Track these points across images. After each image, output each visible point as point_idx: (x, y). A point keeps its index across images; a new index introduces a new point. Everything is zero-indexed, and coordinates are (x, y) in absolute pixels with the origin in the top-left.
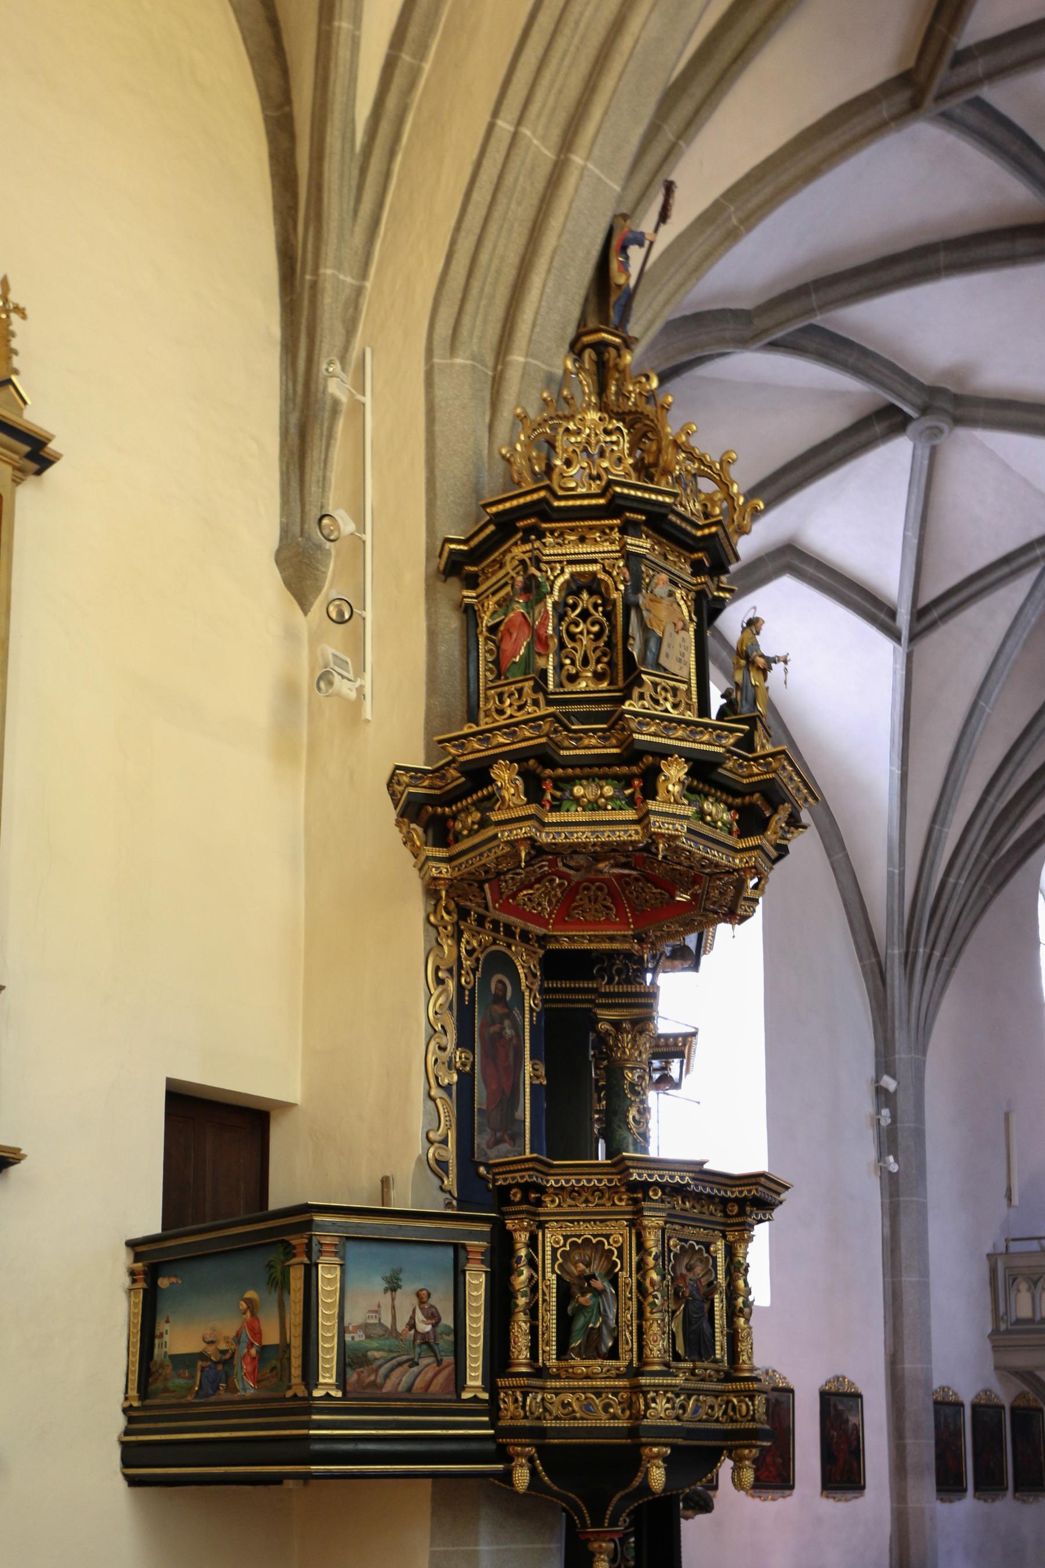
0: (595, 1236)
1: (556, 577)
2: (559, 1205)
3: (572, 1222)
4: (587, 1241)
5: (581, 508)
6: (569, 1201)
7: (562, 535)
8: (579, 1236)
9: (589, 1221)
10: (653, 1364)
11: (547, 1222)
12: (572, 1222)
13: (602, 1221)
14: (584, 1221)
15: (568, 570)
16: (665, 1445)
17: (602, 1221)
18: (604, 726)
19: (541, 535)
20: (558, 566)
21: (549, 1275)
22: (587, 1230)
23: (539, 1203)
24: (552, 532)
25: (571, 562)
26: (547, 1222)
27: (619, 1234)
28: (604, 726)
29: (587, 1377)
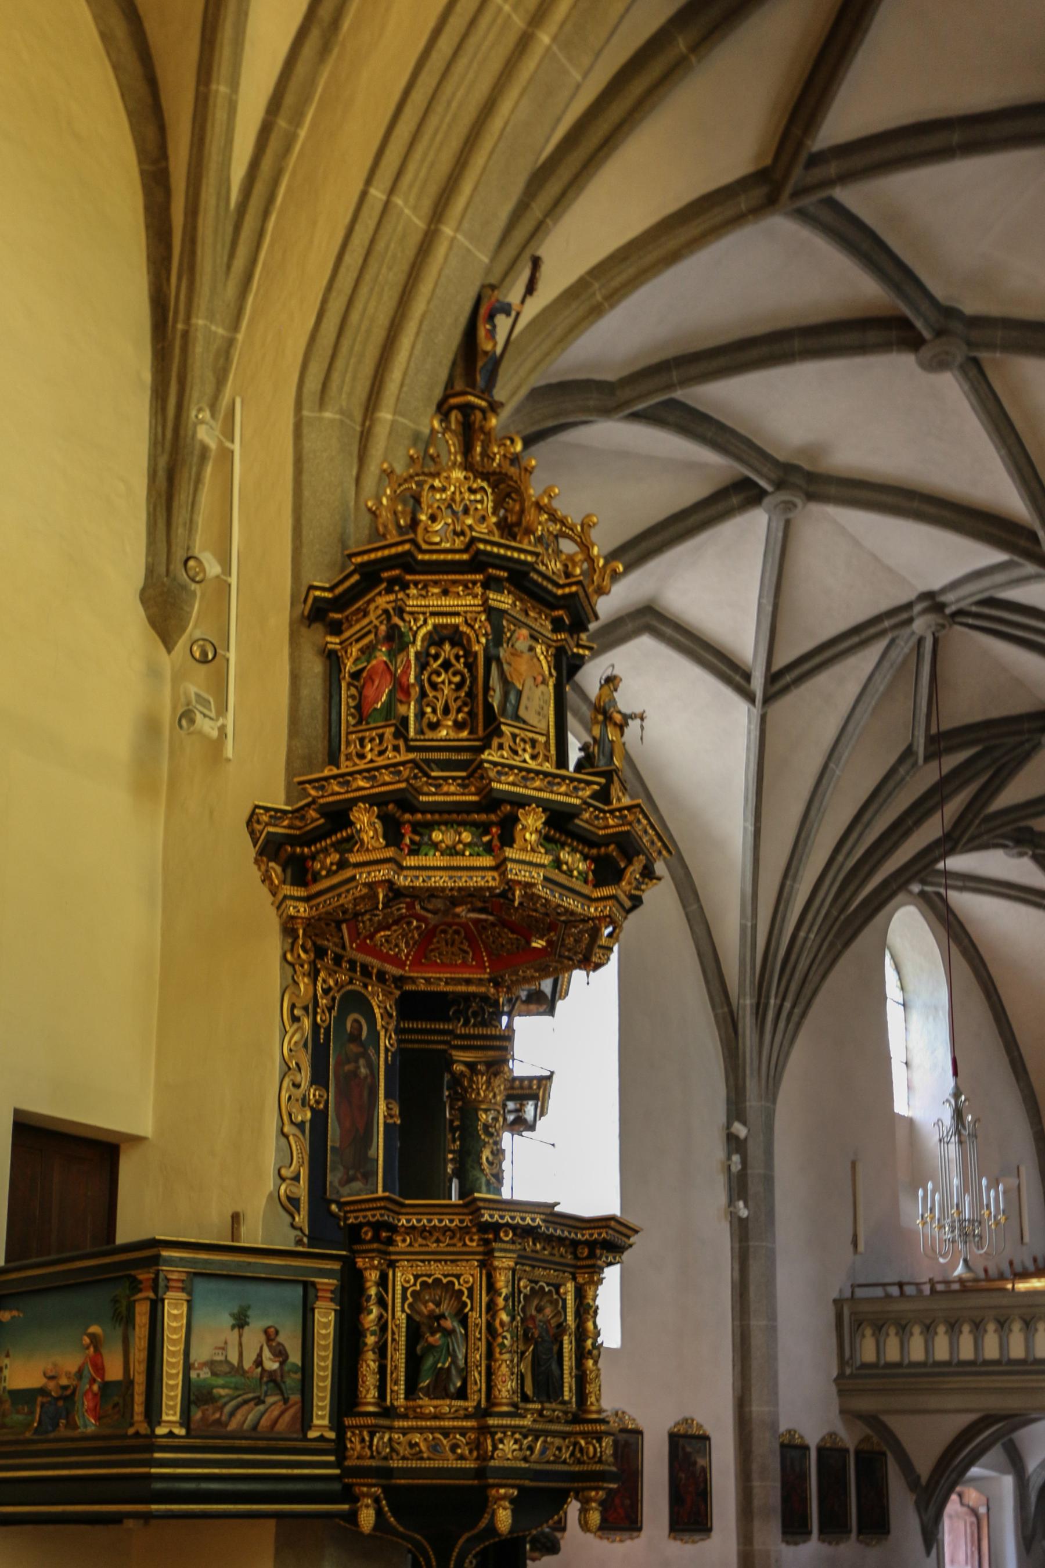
0: (445, 1276)
1: (418, 628)
2: (410, 1245)
3: (423, 1261)
4: (438, 1281)
5: (445, 562)
6: (420, 1240)
7: (425, 587)
8: (429, 1276)
9: (440, 1261)
10: (501, 1404)
11: (397, 1261)
12: (423, 1261)
13: (452, 1261)
14: (435, 1261)
15: (431, 621)
16: (512, 1486)
17: (452, 1261)
18: (464, 774)
19: (405, 586)
20: (422, 618)
21: (398, 1314)
22: (437, 1270)
23: (390, 1242)
24: (416, 584)
25: (433, 614)
26: (397, 1261)
27: (469, 1274)
28: (464, 774)
29: (435, 1417)
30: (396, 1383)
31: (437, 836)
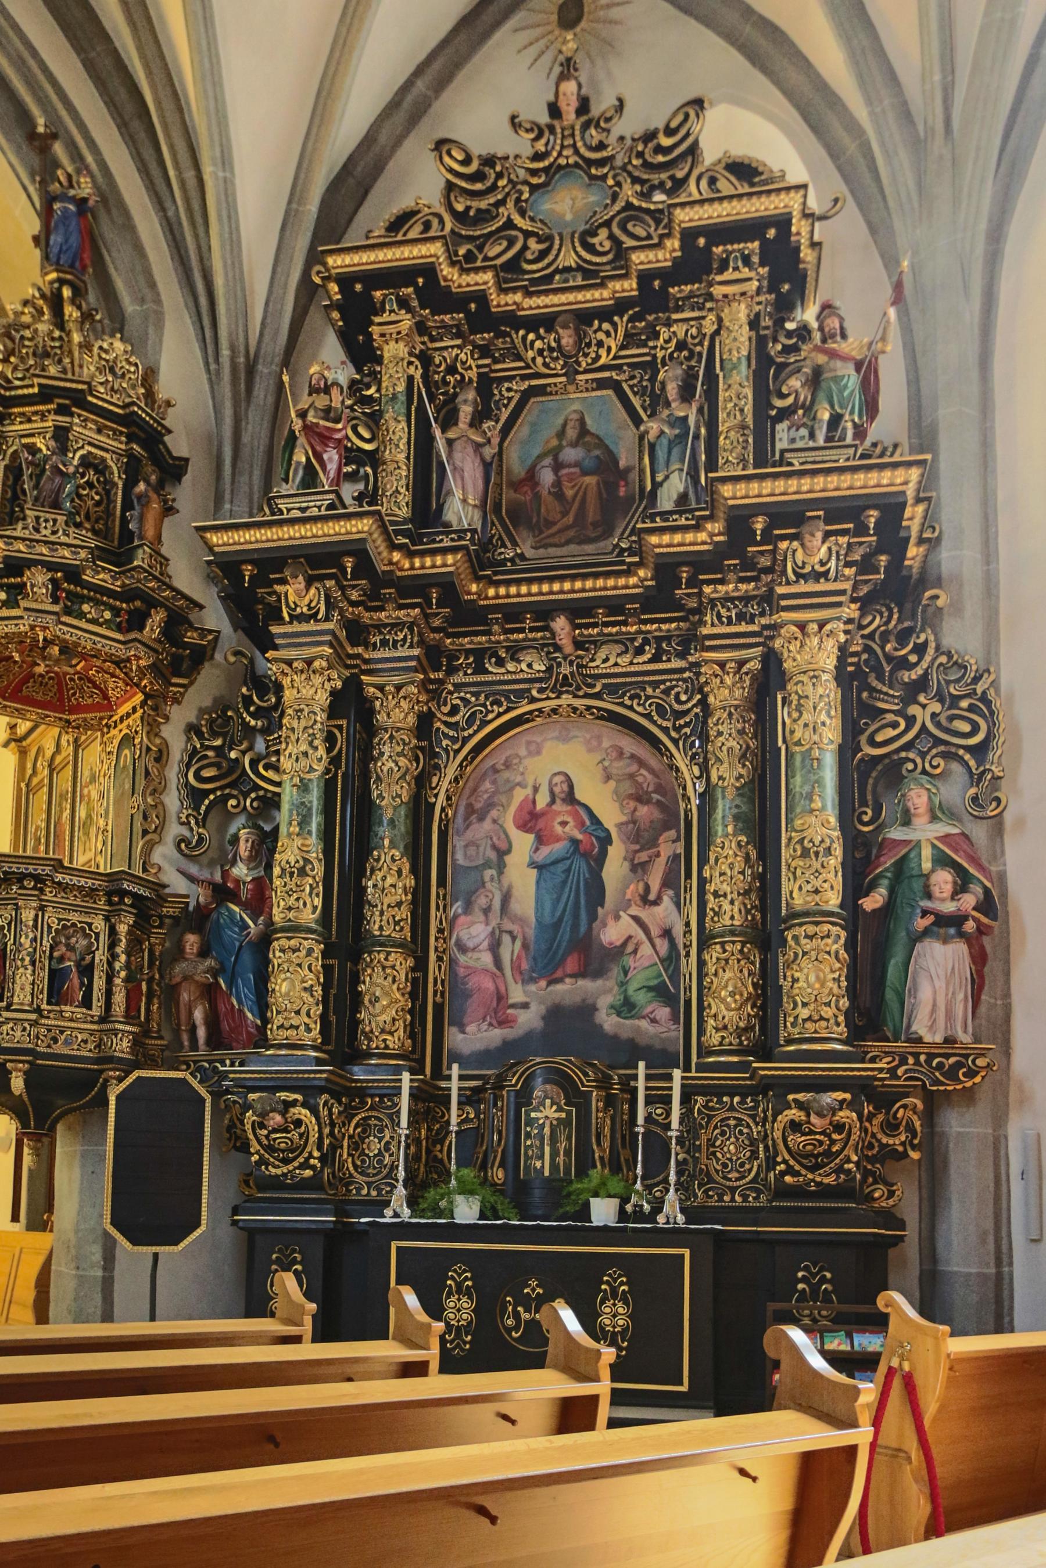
1: (79, 449)
4: (74, 925)
7: (85, 420)
15: (87, 448)
19: (71, 415)
22: (74, 917)
24: (79, 416)
25: (90, 444)
27: (99, 924)
30: (42, 993)
31: (86, 608)
